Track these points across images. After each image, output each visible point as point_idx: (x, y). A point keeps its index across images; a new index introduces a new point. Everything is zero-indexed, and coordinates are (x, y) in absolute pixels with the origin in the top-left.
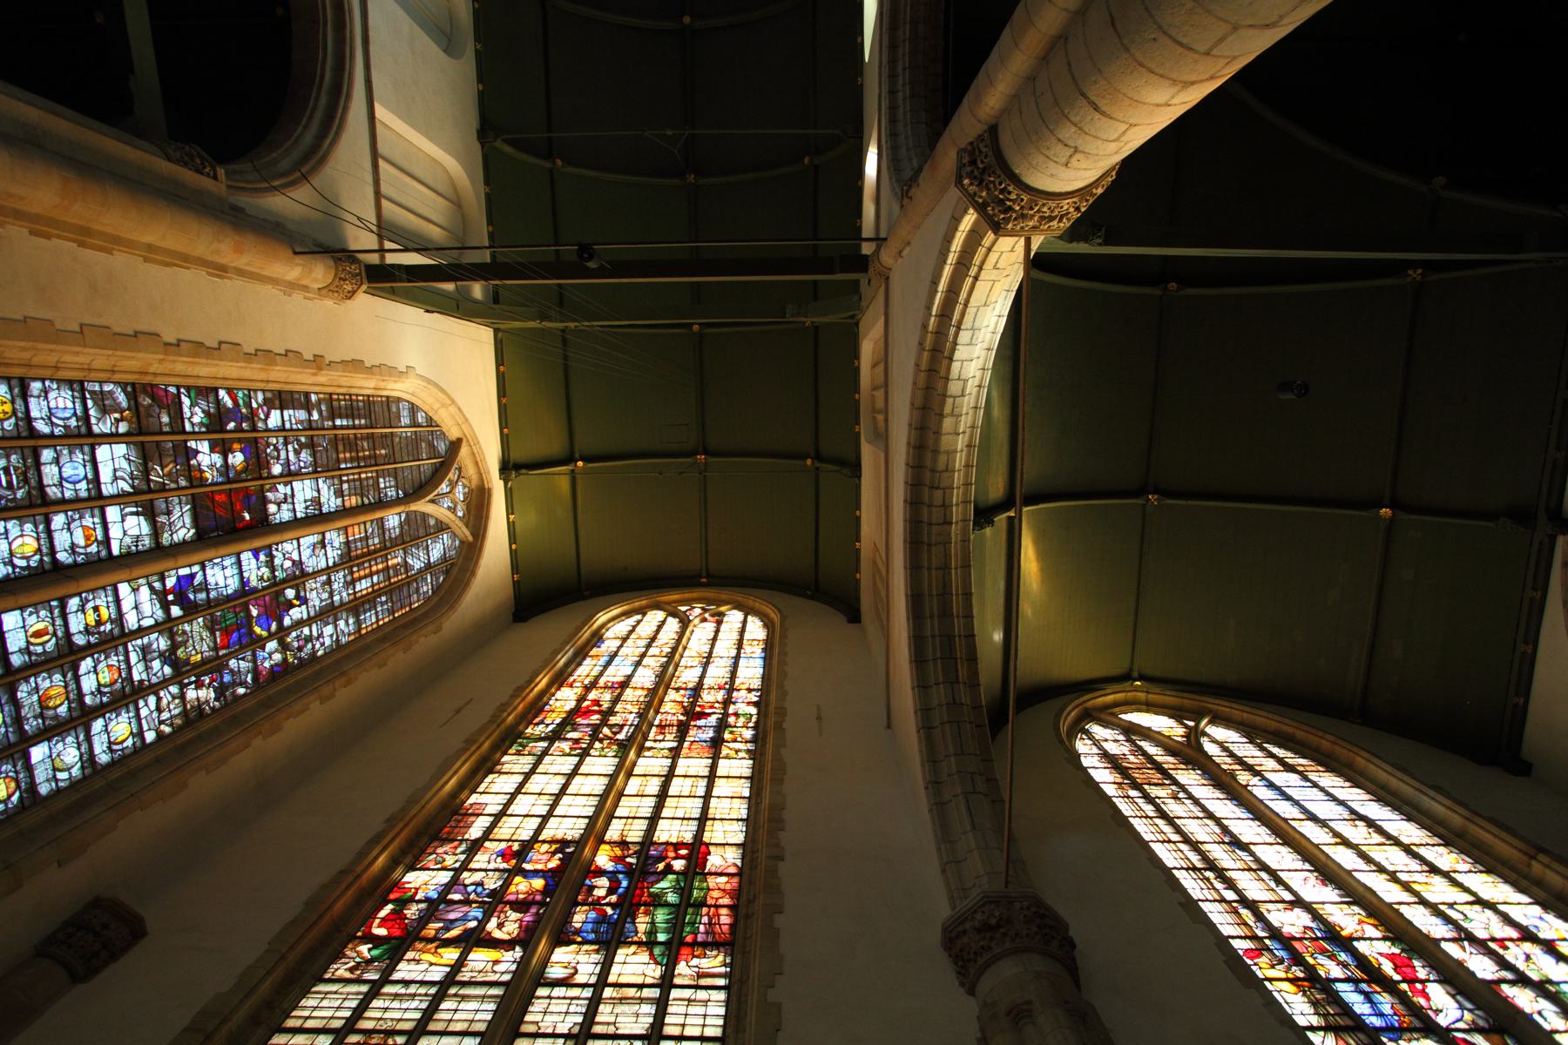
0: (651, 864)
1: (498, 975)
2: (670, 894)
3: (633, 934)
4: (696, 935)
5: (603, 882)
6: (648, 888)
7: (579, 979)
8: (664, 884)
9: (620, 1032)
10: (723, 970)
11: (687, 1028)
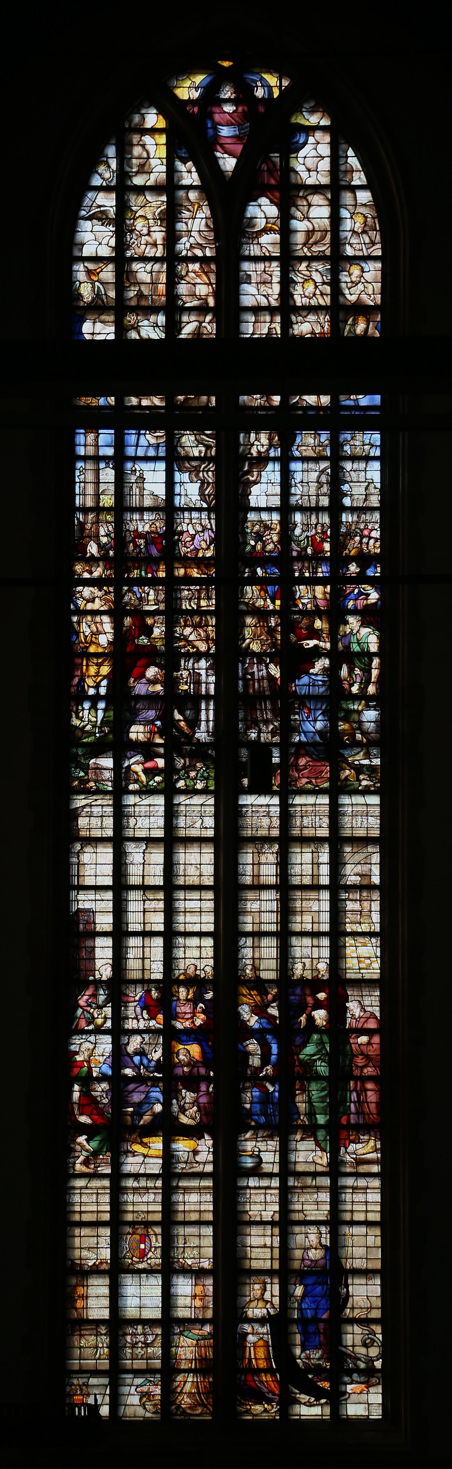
1: (201, 1166)
2: (318, 1063)
3: (296, 1116)
4: (349, 1115)
5: (253, 1046)
7: (267, 1168)
8: (310, 1049)
9: (308, 1218)
10: (374, 1156)
11: (355, 1214)
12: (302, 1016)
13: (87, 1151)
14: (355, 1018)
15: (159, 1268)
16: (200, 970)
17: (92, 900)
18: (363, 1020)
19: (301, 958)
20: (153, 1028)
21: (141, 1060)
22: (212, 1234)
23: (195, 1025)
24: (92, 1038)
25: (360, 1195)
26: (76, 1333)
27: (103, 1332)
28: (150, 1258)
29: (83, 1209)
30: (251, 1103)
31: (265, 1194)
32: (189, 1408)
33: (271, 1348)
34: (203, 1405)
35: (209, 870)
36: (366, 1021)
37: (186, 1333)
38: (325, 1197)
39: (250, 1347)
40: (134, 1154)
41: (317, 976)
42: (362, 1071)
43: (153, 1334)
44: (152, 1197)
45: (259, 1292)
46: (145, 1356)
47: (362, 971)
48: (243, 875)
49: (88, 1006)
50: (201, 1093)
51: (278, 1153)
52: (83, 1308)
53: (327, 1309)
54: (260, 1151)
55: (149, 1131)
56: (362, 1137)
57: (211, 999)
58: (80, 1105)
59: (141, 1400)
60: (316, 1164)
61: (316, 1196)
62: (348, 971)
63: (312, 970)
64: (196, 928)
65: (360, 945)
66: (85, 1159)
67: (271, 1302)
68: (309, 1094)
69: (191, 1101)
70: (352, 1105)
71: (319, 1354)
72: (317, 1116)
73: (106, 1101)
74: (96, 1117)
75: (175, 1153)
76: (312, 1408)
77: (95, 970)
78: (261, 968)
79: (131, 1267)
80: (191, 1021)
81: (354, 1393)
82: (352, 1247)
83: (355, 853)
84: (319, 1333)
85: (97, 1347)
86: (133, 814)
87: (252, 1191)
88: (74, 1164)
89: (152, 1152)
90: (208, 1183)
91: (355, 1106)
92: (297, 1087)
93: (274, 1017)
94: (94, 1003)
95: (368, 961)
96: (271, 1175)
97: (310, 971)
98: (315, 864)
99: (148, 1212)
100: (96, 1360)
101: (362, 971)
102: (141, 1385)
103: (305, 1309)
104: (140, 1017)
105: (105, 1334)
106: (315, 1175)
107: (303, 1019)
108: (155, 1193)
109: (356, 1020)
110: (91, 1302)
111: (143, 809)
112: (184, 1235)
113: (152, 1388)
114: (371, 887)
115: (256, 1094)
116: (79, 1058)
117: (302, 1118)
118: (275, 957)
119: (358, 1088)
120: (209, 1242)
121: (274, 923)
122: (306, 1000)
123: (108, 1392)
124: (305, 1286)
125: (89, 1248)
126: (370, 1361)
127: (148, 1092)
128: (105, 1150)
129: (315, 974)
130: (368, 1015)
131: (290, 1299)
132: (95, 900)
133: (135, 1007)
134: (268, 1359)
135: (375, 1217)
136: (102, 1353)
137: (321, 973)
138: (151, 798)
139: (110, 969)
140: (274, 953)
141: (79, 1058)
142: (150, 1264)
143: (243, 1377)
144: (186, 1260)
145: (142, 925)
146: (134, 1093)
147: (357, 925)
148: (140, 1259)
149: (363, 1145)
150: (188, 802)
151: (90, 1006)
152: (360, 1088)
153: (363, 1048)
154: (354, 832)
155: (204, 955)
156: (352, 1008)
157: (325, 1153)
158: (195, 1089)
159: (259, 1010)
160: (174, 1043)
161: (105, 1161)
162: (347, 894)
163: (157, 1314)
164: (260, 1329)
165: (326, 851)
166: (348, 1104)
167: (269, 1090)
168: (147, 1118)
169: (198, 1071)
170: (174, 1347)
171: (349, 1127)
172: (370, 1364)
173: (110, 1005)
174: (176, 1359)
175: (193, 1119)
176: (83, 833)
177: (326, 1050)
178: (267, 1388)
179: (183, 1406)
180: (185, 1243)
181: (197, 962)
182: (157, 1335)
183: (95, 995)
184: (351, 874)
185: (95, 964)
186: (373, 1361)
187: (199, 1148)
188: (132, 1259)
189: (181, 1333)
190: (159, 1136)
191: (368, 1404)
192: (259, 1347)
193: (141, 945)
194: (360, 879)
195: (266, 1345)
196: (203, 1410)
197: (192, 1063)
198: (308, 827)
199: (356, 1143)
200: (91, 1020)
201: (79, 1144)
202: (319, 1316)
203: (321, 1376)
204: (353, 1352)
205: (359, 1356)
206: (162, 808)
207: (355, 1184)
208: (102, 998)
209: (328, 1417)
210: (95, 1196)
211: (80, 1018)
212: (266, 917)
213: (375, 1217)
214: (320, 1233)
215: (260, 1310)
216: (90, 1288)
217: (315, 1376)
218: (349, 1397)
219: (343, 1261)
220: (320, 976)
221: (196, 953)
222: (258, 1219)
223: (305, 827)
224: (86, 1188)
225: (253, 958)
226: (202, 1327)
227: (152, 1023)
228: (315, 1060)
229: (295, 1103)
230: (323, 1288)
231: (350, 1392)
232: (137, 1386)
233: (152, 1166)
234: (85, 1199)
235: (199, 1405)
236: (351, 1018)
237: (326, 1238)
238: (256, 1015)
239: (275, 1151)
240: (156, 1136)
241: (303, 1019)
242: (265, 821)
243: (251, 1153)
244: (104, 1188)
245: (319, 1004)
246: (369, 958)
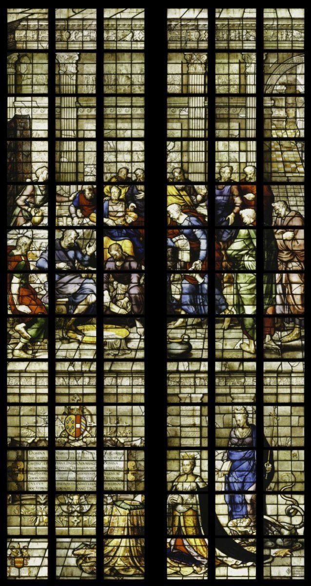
0: (221, 216)
1: (133, 353)
2: (246, 258)
3: (224, 307)
5: (182, 242)
6: (226, 249)
7: (196, 354)
8: (237, 245)
9: (236, 401)
12: (230, 214)
13: (25, 338)
14: (280, 217)
15: (95, 446)
16: (131, 173)
17: (29, 107)
18: (288, 219)
19: (229, 162)
20: (87, 225)
21: (76, 255)
22: (144, 414)
23: (126, 223)
24: (29, 233)
25: (285, 379)
26: (17, 503)
27: (43, 502)
28: (86, 437)
29: (23, 391)
30: (181, 294)
31: (195, 378)
32: (122, 570)
33: (200, 517)
34: (137, 567)
35: (139, 79)
36: (291, 219)
37: (119, 503)
38: (251, 381)
39: (179, 517)
40: (69, 340)
41: (245, 179)
42: (287, 266)
43: (88, 504)
44: (87, 380)
45: (188, 468)
46: (80, 524)
47: (288, 175)
48: (173, 84)
49: (25, 205)
50: (132, 285)
51: (207, 340)
52: (23, 481)
53: (253, 483)
54: (189, 338)
55: (84, 318)
56: (287, 325)
57: (142, 199)
58: (19, 296)
59: (77, 561)
60: (244, 351)
61: (243, 380)
62: (274, 175)
63: (240, 173)
64: (128, 134)
65: (285, 149)
66: (23, 346)
67: (200, 477)
68: (237, 286)
69: (122, 292)
70: (278, 297)
71: (246, 522)
72: (245, 307)
73: (44, 292)
74: (34, 307)
75: (108, 341)
76: (239, 570)
77: (32, 173)
78: (190, 171)
79: (68, 445)
80: (122, 219)
81: (278, 556)
82: (278, 426)
83: (280, 64)
84: (246, 503)
85: (36, 515)
86: (66, 28)
87: (182, 376)
88: (13, 350)
89: (86, 339)
90: (140, 367)
91: (281, 298)
92: (225, 280)
93: (203, 216)
94: (31, 203)
95: (293, 166)
96: (200, 360)
97: (238, 175)
98: (243, 74)
99: (83, 394)
100: (36, 526)
101: (288, 175)
102: (77, 549)
103: (233, 482)
104: (74, 215)
105: (44, 504)
106: (242, 360)
107: (231, 217)
108: (90, 377)
109: (282, 219)
110: (31, 476)
111: (76, 23)
112: (117, 416)
113: (88, 552)
114: (297, 95)
115: (186, 285)
116: (16, 252)
117: (230, 308)
118: (204, 161)
119: (284, 281)
120: (141, 421)
121: (202, 130)
122: (234, 200)
123: (47, 555)
124: (233, 461)
125: (28, 426)
126: (295, 528)
127: (82, 284)
128: (42, 337)
129: (242, 177)
130: (292, 214)
131: (218, 474)
132: (32, 107)
133: (69, 206)
134: (197, 527)
135: (299, 399)
136: (41, 520)
137: (249, 176)
138: (85, 11)
139: (46, 172)
140: (202, 157)
141: (16, 252)
142: (85, 442)
143: (173, 542)
144: (119, 439)
145: (75, 132)
146: (69, 285)
147: (283, 131)
148: (76, 437)
149: (289, 332)
150: (118, 16)
151: (27, 204)
152: (286, 281)
153: (289, 244)
154: (279, 45)
155: (135, 158)
156: (277, 207)
157: (252, 341)
158: (128, 282)
159: (189, 209)
160: (105, 239)
161: (42, 347)
162: (273, 102)
163: (92, 487)
164: (189, 499)
165: (254, 62)
166: (274, 296)
167: (198, 282)
168: (81, 308)
169: (130, 265)
170: (107, 515)
171: (275, 315)
172: (293, 531)
173: (47, 204)
174: (109, 527)
175: (124, 308)
176: (20, 46)
177: (254, 245)
178: (197, 552)
179: (117, 568)
180: (118, 423)
181: (129, 166)
182: (92, 505)
183: (33, 195)
184: (276, 82)
185: (31, 167)
186: (296, 529)
187: (131, 336)
188: (68, 437)
189: (114, 504)
190: (93, 324)
191: (292, 567)
192: (188, 516)
193: (75, 149)
194: (285, 88)
195: (196, 514)
196: (135, 572)
197: (124, 258)
198: (235, 40)
199: (281, 331)
200: (29, 218)
201: (18, 331)
202: (246, 488)
203: (248, 541)
204: (277, 520)
205: (283, 524)
206: (95, 23)
207: (280, 369)
208: (39, 199)
209: (255, 578)
210: (33, 379)
211: (18, 216)
212: (194, 124)
213: (300, 399)
214: (247, 413)
215: (189, 484)
216: (30, 463)
217: (242, 541)
218: (273, 560)
219: (269, 439)
220: (248, 179)
221: (127, 157)
222: (188, 401)
223: (232, 40)
224: (25, 371)
225: (182, 162)
226: (134, 498)
227: (86, 220)
228: (243, 255)
229: (222, 295)
230: (250, 464)
231: (274, 555)
232: (74, 550)
233: (86, 352)
234: (24, 381)
235: (132, 567)
236: (277, 217)
237: (252, 418)
238: (185, 213)
239: (204, 339)
240: (90, 324)
241: (231, 217)
242: (194, 35)
243: (181, 340)
244: (43, 372)
245: (245, 205)
246: (295, 162)
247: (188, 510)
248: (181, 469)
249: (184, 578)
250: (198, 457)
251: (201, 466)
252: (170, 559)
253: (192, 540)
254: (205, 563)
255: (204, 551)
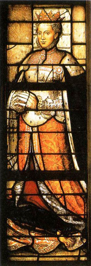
33: (70, 135)
39: (31, 133)
67: (71, 54)
143: (19, 188)
164: (50, 101)
178: (65, 207)
215: (49, 69)
247: (48, 120)
248: (35, 41)
249: (41, 259)
250: (67, 17)
251: (72, 35)
252: (13, 221)
253: (55, 185)
254: (81, 229)
255: (80, 206)
